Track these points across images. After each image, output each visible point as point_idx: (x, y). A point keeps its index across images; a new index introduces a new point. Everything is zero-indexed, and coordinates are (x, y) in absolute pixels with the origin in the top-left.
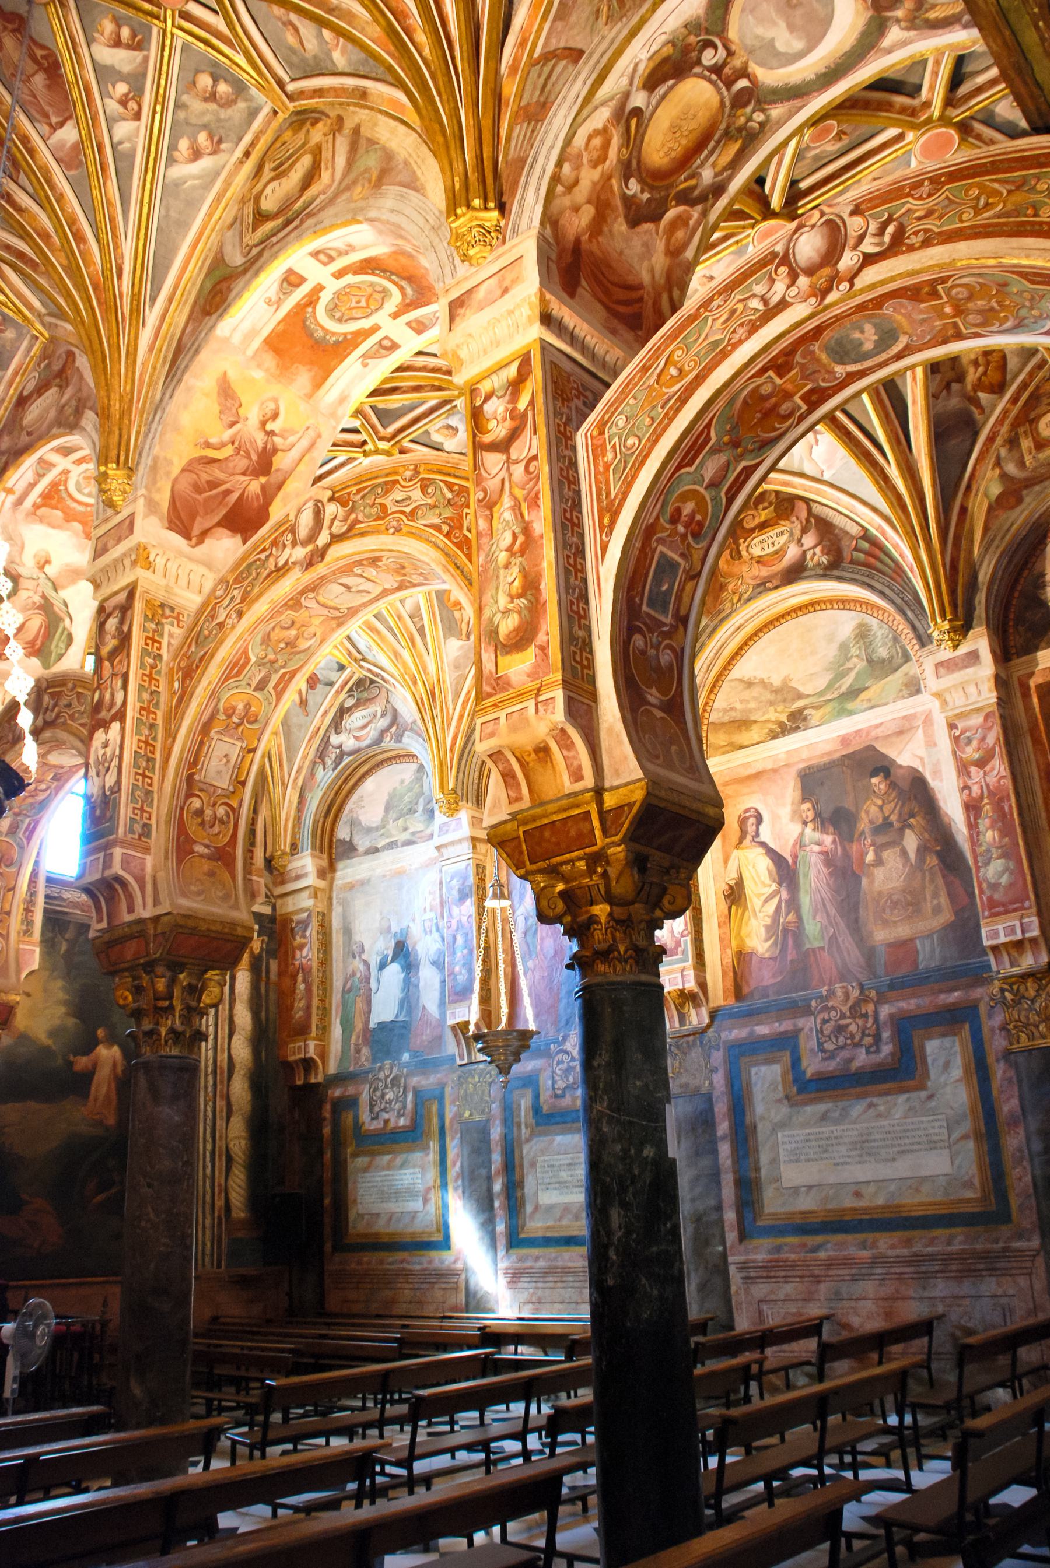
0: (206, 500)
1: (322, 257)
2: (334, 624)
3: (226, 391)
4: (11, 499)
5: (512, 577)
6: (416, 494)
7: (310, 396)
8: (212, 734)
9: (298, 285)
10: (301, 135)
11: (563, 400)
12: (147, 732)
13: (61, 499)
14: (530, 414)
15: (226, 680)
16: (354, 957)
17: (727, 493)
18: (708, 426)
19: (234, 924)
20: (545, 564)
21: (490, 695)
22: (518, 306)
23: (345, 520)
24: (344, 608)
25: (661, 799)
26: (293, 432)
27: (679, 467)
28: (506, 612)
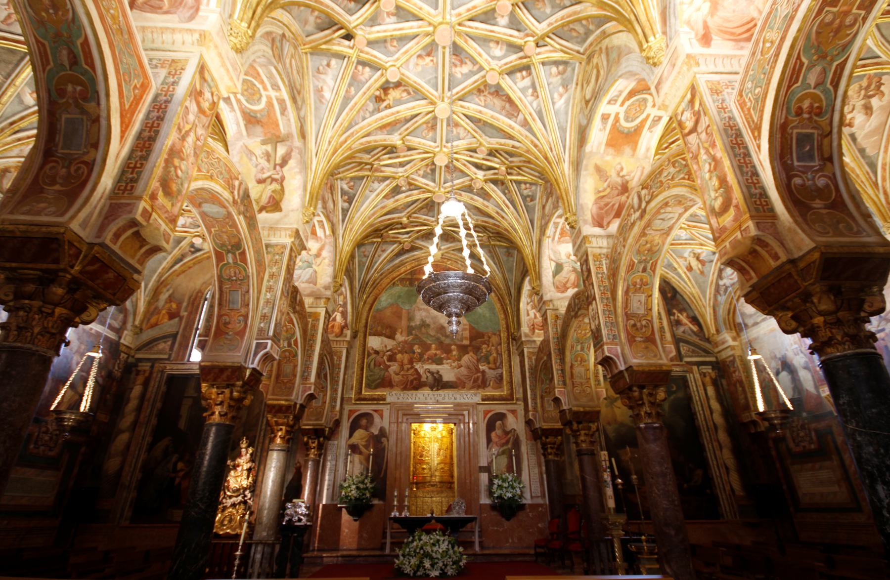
0: (606, 212)
1: (612, 102)
2: (665, 236)
3: (599, 170)
4: (550, 239)
5: (715, 182)
6: (672, 170)
7: (633, 155)
8: (630, 294)
9: (608, 118)
10: (591, 64)
11: (718, 94)
12: (605, 301)
13: (566, 233)
14: (701, 109)
15: (628, 272)
16: (762, 372)
17: (831, 83)
18: (799, 57)
19: (661, 365)
20: (726, 169)
21: (719, 237)
22: (681, 68)
23: (649, 194)
24: (666, 228)
25: (835, 253)
26: (632, 172)
27: (789, 87)
28: (716, 198)
